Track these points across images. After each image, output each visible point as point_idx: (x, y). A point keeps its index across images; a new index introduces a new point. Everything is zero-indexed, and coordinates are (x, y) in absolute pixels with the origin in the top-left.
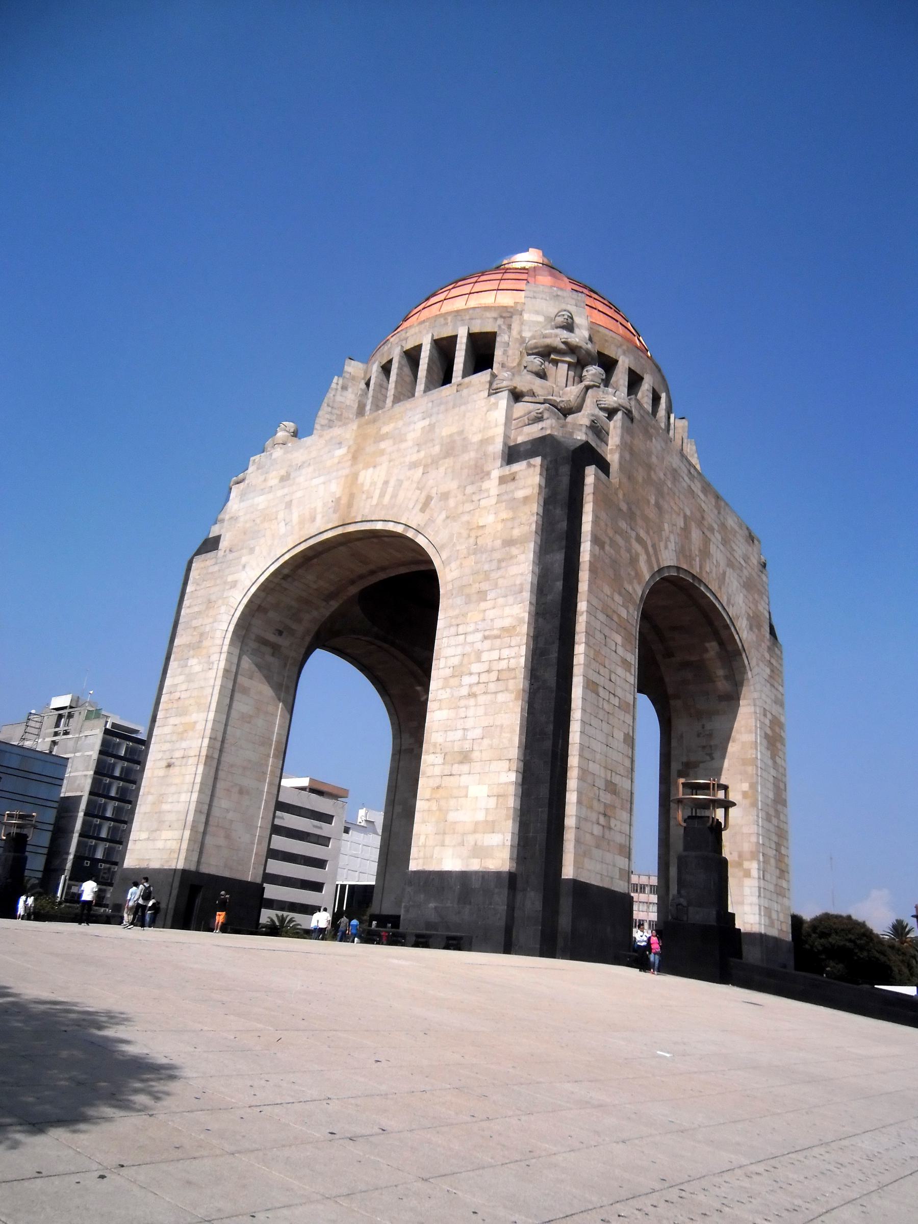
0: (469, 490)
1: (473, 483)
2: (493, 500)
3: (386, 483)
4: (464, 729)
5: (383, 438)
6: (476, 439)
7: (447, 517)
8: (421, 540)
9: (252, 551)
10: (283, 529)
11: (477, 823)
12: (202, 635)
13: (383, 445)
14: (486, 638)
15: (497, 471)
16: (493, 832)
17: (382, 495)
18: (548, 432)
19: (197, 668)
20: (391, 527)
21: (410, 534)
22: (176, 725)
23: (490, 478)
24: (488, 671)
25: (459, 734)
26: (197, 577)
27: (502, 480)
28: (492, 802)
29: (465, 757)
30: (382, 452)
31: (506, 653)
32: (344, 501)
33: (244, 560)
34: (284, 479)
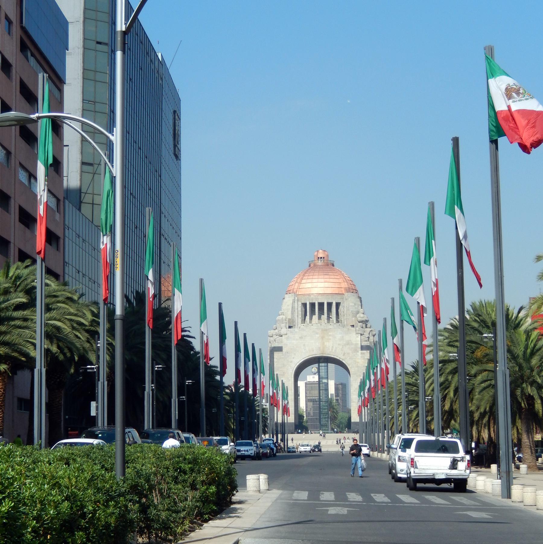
0: (354, 353)
1: (355, 352)
2: (360, 357)
3: (333, 347)
5: (330, 335)
6: (354, 343)
7: (350, 358)
8: (344, 362)
9: (295, 354)
12: (284, 373)
13: (330, 337)
15: (360, 352)
17: (332, 349)
18: (369, 345)
21: (341, 360)
27: (362, 353)
30: (330, 339)
34: (301, 338)
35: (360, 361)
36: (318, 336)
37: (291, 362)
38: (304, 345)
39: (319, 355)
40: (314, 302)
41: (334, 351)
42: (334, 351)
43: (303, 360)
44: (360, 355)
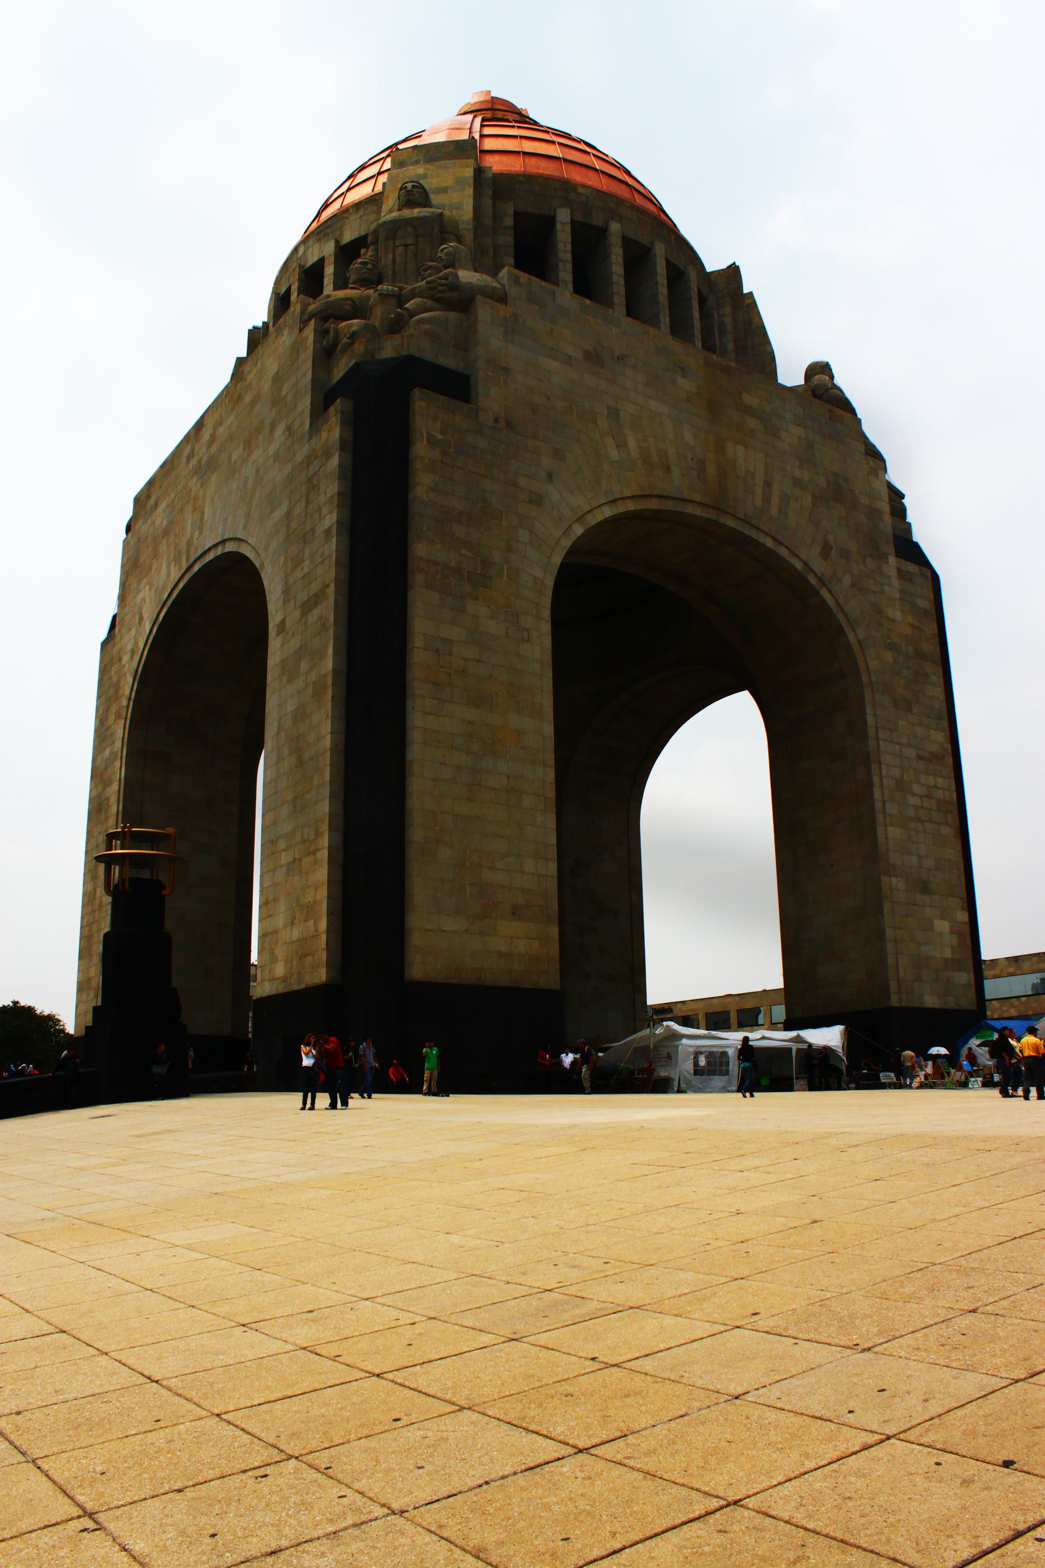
2: (897, 595)
3: (768, 484)
4: (919, 856)
7: (853, 585)
8: (824, 592)
9: (558, 455)
10: (614, 454)
11: (946, 960)
14: (920, 758)
15: (892, 560)
16: (960, 971)
17: (766, 499)
19: (494, 627)
20: (784, 552)
21: (813, 581)
22: (470, 723)
23: (887, 563)
24: (929, 796)
25: (915, 860)
26: (440, 437)
28: (954, 940)
29: (925, 888)
31: (940, 782)
32: (711, 470)
33: (546, 462)
35: (898, 615)
36: (685, 384)
37: (537, 500)
38: (614, 414)
39: (698, 511)
40: (597, 220)
41: (774, 510)
42: (774, 510)
43: (607, 512)
44: (895, 582)
